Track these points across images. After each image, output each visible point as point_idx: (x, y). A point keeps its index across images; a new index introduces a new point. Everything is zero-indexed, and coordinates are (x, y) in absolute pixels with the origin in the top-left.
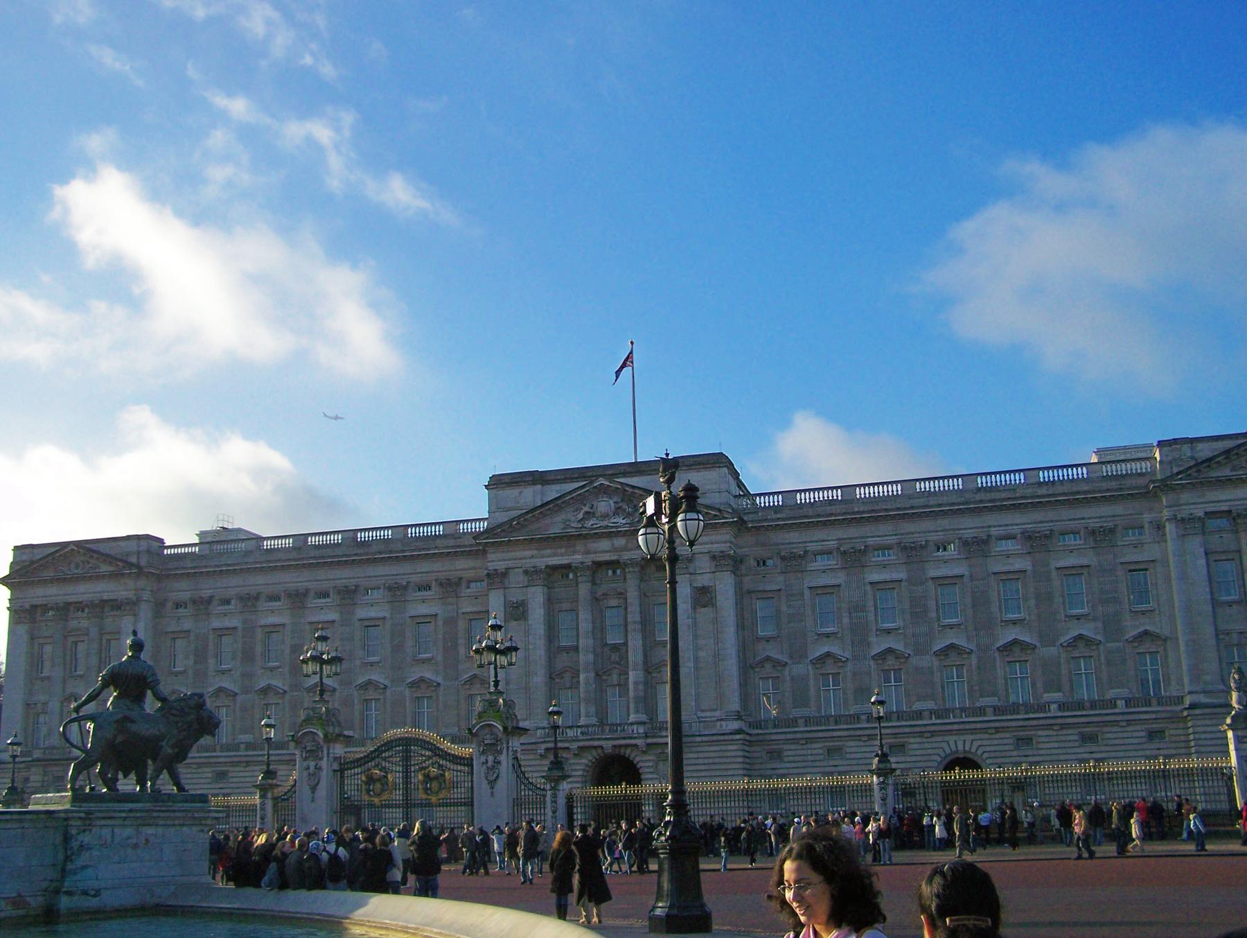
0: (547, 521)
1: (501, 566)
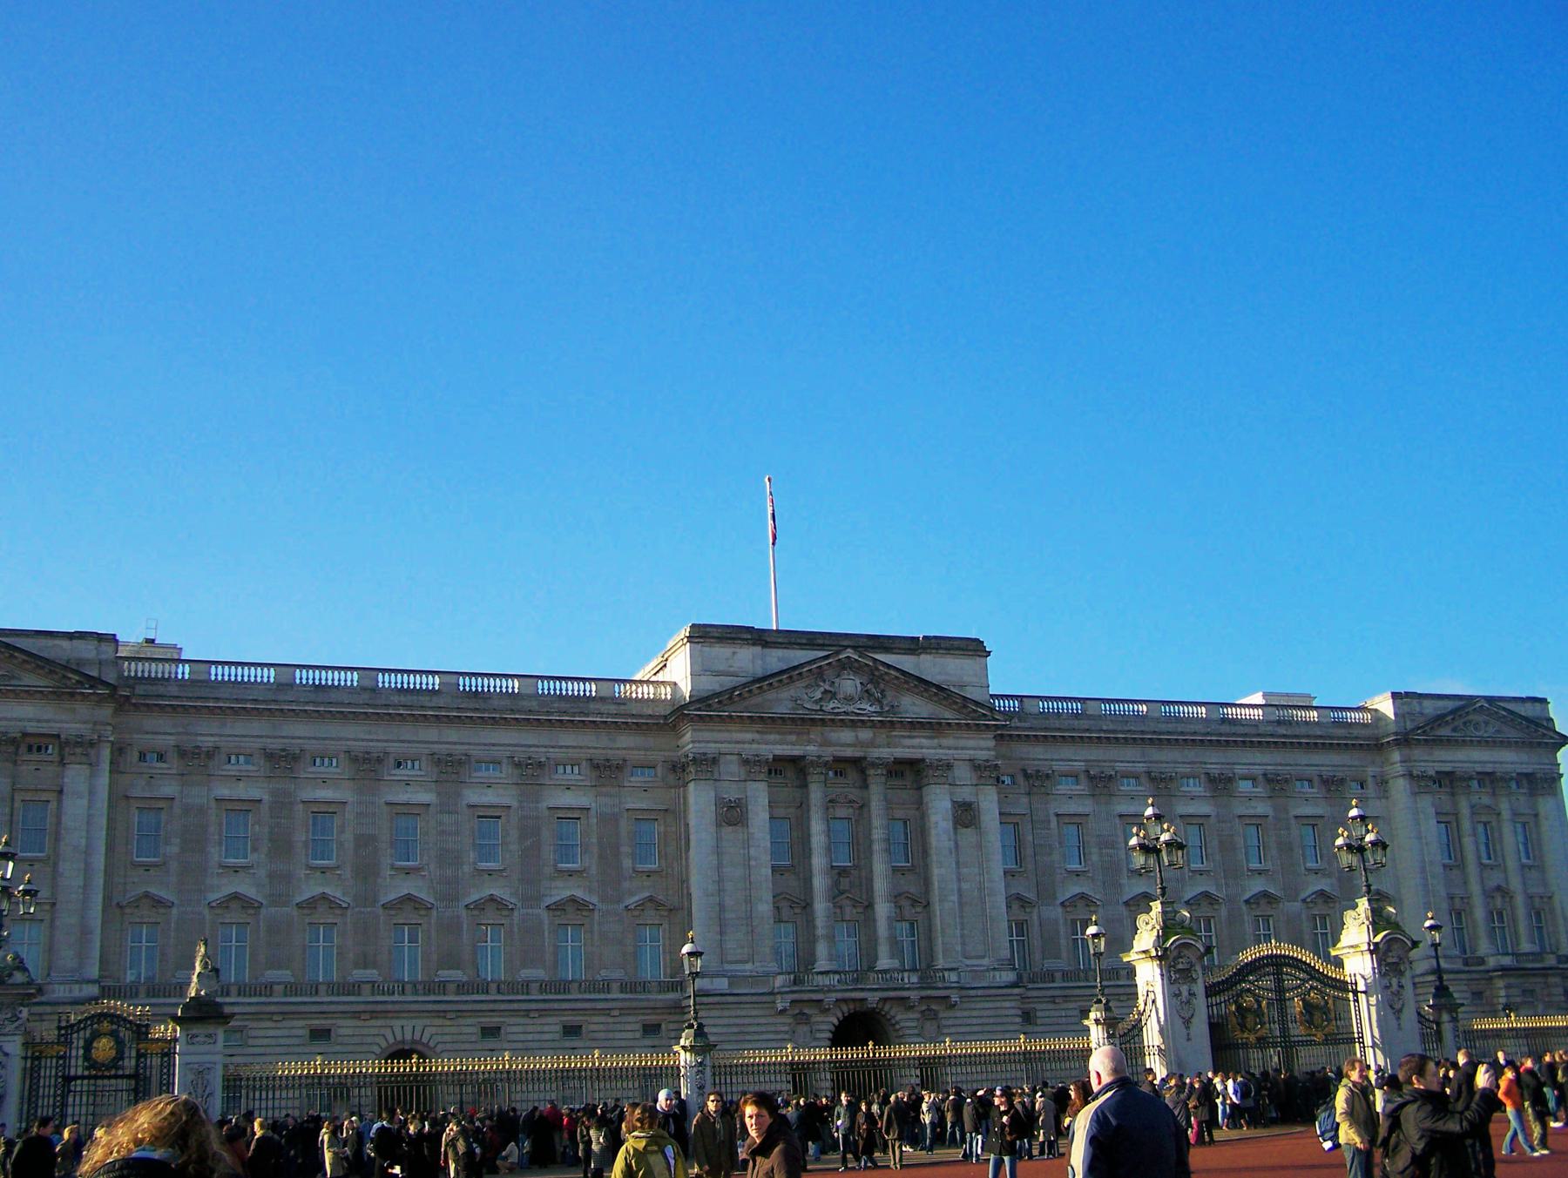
0: (771, 695)
1: (712, 748)
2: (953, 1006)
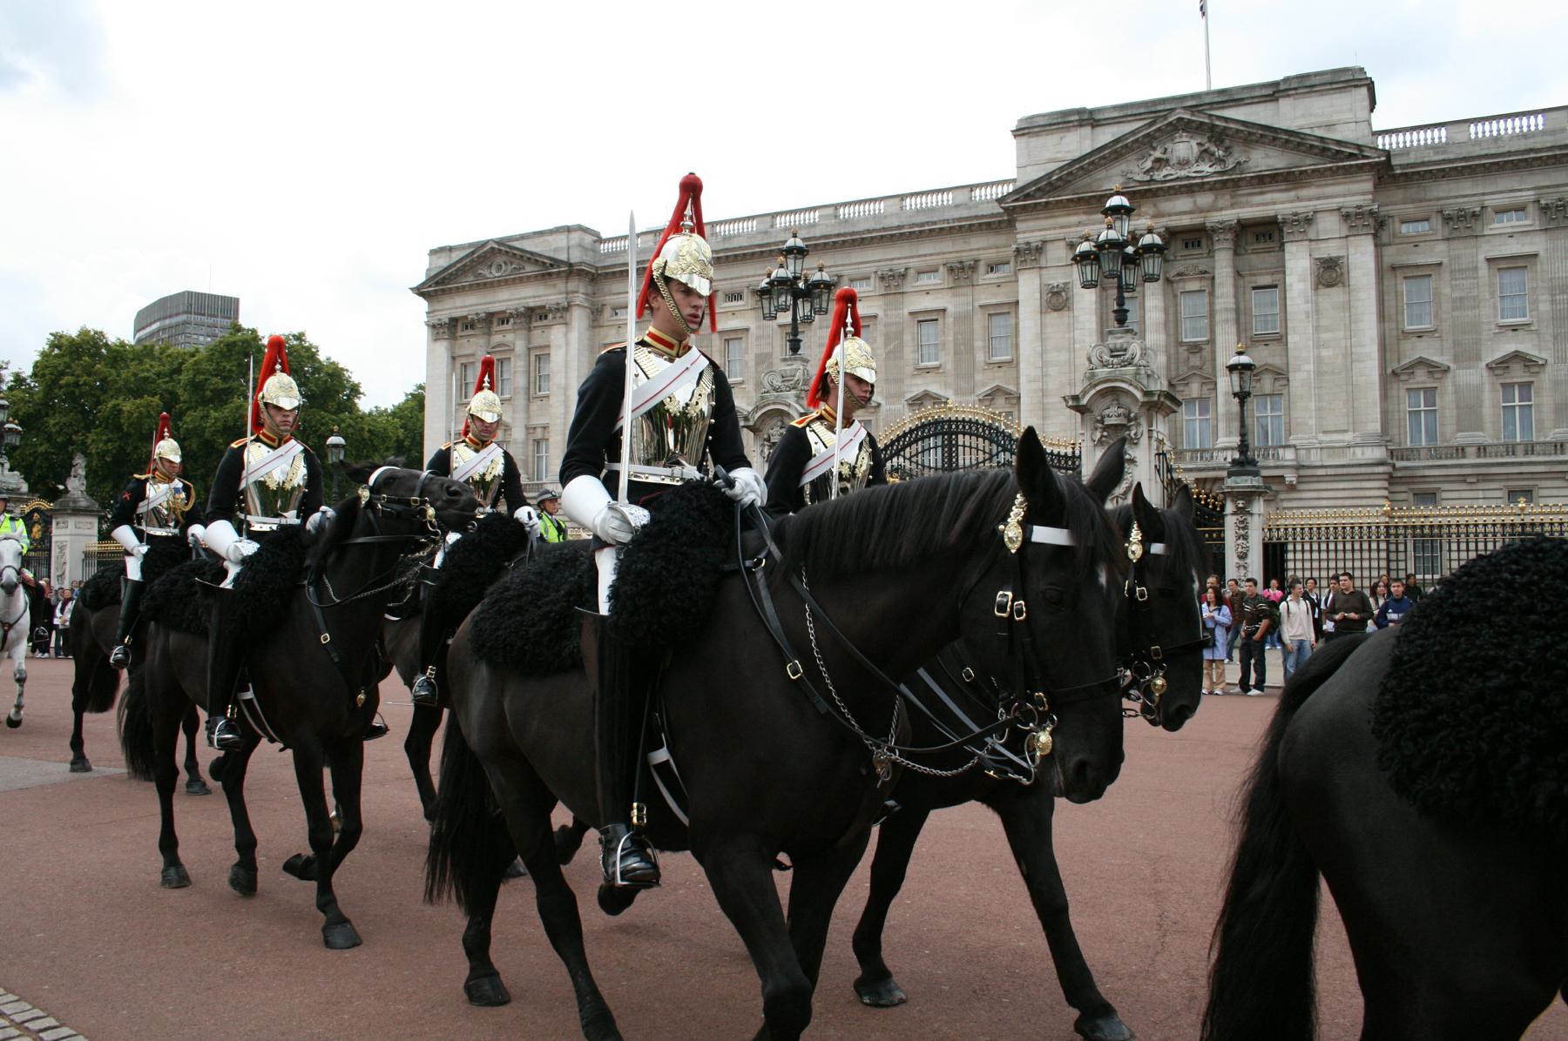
0: (1101, 174)
1: (1034, 238)
2: (1292, 488)
